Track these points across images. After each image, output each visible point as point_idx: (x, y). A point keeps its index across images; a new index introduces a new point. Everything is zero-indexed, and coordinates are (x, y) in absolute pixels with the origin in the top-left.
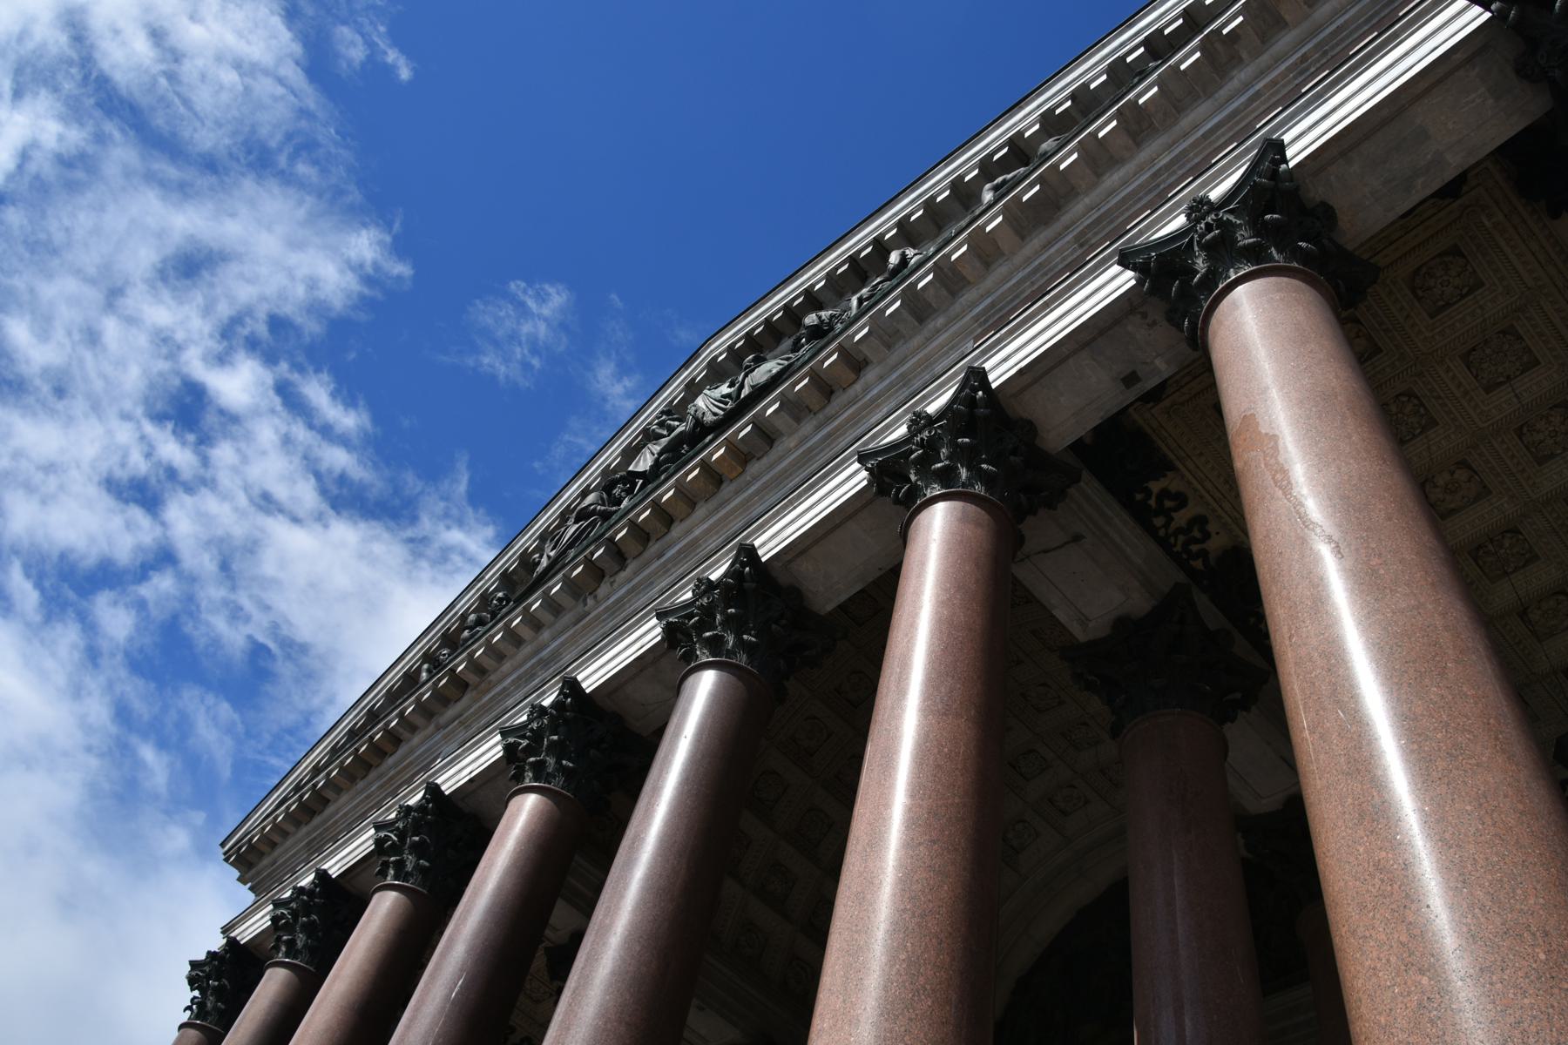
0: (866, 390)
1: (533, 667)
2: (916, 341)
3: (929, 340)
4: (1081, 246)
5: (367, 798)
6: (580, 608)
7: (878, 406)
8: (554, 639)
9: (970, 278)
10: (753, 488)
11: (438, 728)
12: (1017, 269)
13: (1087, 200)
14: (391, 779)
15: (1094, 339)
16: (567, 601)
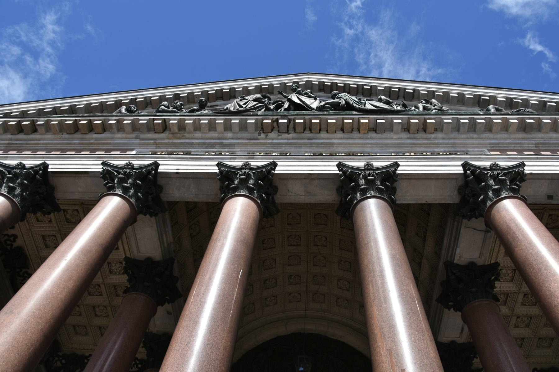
0: (435, 139)
1: (215, 143)
2: (463, 136)
3: (468, 139)
4: (536, 147)
5: (68, 144)
6: (256, 135)
7: (439, 147)
8: (233, 139)
9: (493, 131)
10: (372, 142)
11: (137, 138)
12: (510, 139)
13: (543, 135)
14: (91, 143)
15: (555, 179)
16: (251, 129)
